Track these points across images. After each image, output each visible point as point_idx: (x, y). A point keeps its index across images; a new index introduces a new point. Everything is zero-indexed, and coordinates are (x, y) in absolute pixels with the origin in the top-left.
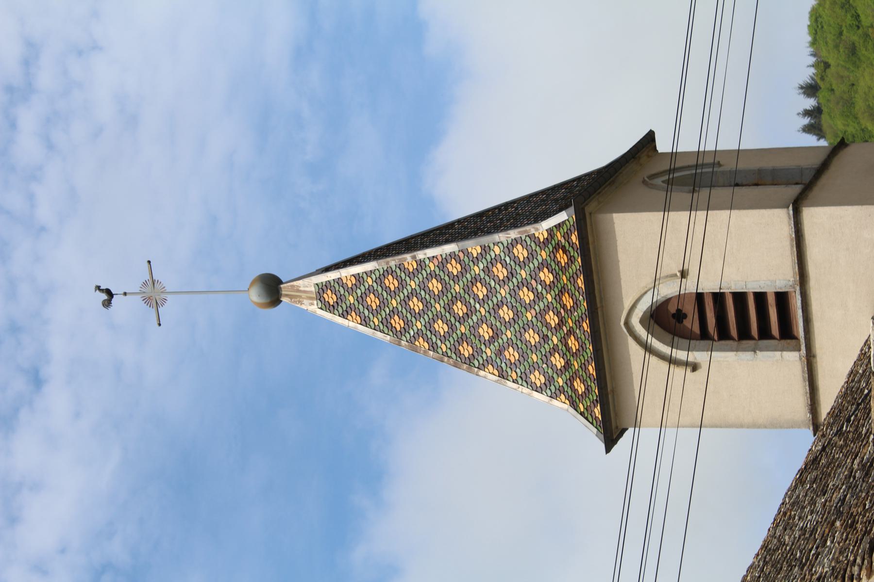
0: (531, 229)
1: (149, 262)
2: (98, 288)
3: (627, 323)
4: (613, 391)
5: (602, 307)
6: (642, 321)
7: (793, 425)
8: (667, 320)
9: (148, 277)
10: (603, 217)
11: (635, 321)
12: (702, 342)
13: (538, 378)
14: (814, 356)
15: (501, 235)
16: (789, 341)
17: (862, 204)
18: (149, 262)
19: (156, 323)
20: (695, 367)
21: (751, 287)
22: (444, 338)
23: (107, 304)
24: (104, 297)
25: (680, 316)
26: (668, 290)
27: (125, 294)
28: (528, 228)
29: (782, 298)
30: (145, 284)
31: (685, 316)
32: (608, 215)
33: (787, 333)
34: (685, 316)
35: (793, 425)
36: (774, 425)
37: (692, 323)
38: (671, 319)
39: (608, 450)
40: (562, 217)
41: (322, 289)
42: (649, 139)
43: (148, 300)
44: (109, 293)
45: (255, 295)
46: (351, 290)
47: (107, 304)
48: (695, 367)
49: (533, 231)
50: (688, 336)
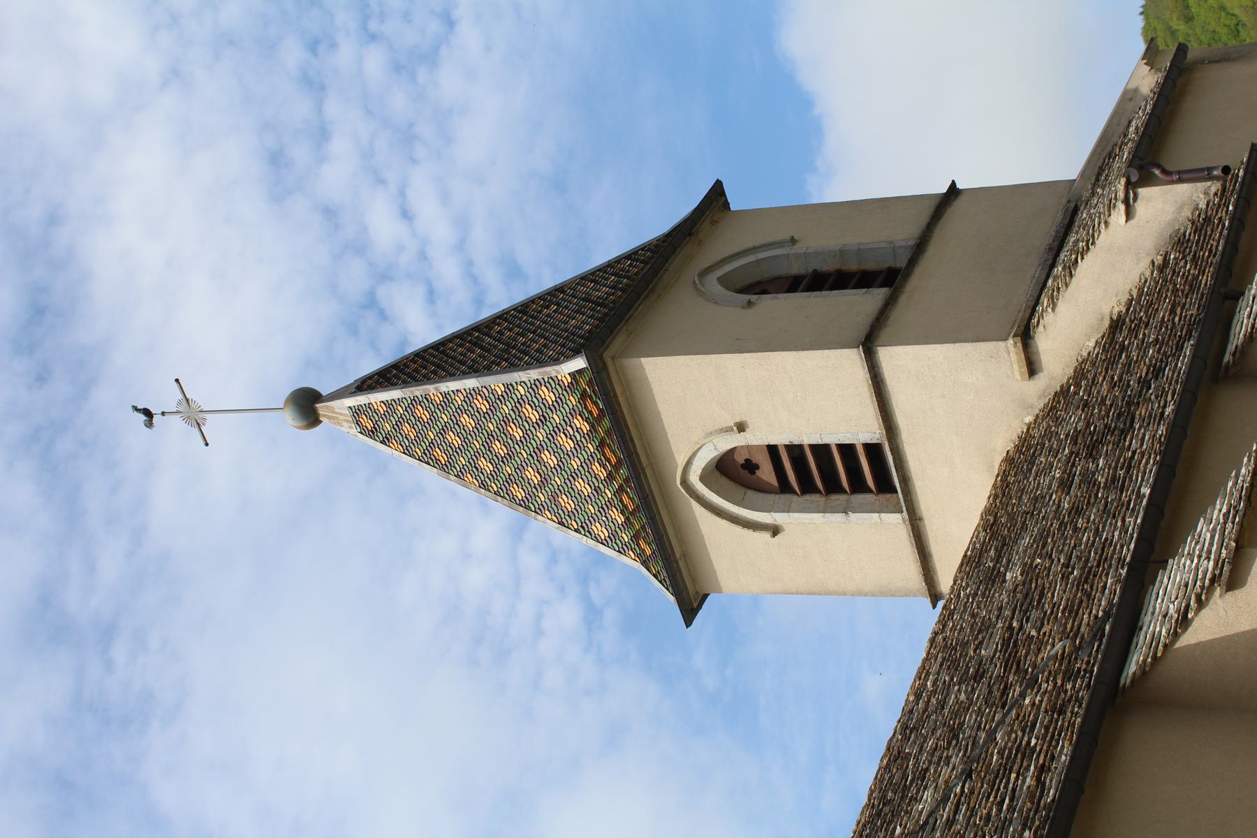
0: (551, 370)
1: (177, 380)
2: (136, 409)
3: (685, 482)
4: (684, 555)
5: (651, 464)
6: (703, 479)
7: (907, 593)
8: (734, 472)
9: (181, 396)
10: (630, 362)
11: (694, 478)
12: (782, 496)
13: (597, 529)
14: (921, 519)
15: (521, 373)
16: (888, 496)
17: (954, 342)
18: (177, 380)
19: (203, 443)
20: (775, 531)
21: (833, 436)
22: (492, 477)
23: (149, 424)
24: (143, 418)
25: (750, 466)
26: (725, 444)
27: (163, 414)
28: (548, 369)
29: (873, 450)
30: (179, 403)
31: (757, 467)
32: (634, 361)
33: (884, 485)
34: (757, 467)
35: (907, 593)
36: (883, 593)
37: (767, 473)
38: (741, 471)
39: (688, 623)
40: (579, 363)
41: (357, 412)
42: (717, 191)
43: (188, 419)
44: (148, 413)
45: (289, 420)
46: (385, 416)
47: (149, 424)
48: (775, 531)
49: (554, 374)
50: (762, 488)
